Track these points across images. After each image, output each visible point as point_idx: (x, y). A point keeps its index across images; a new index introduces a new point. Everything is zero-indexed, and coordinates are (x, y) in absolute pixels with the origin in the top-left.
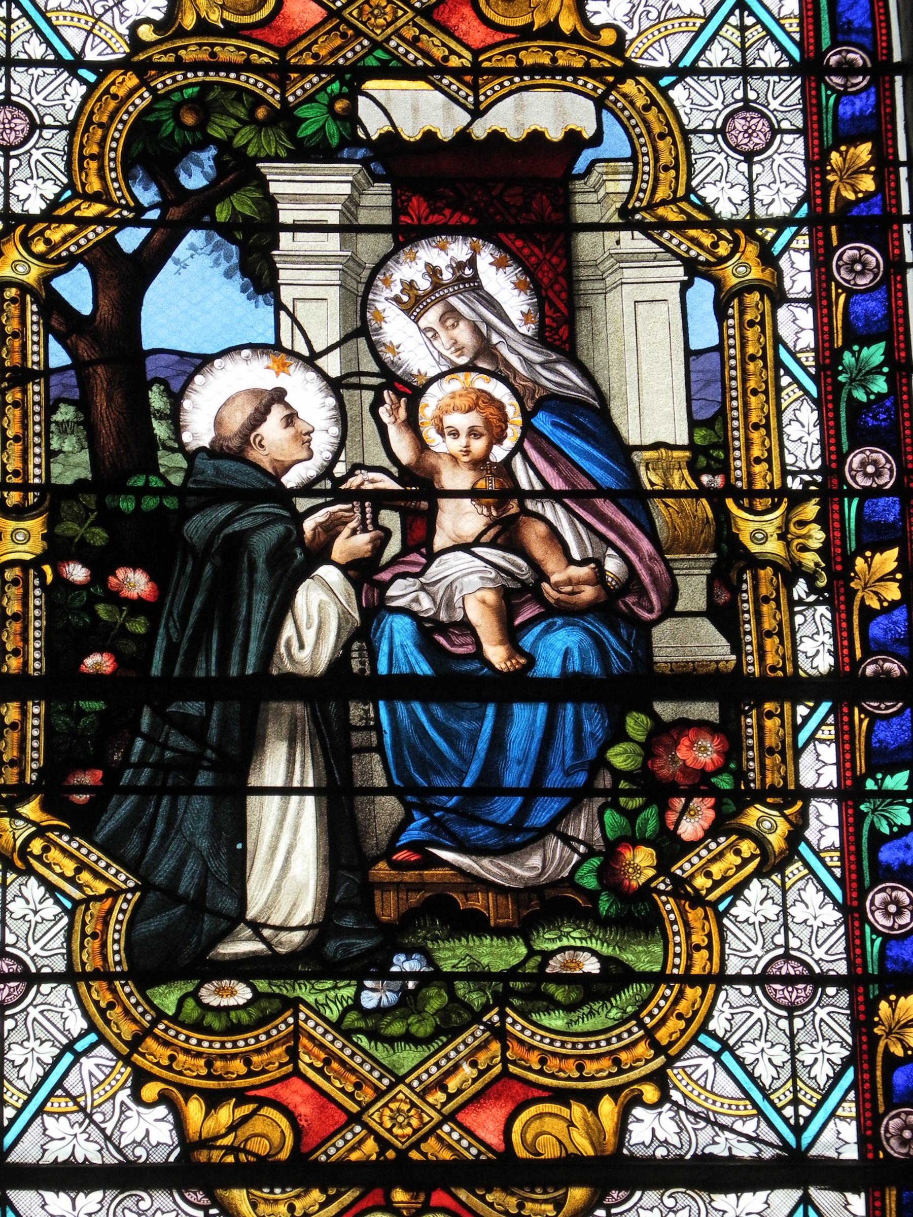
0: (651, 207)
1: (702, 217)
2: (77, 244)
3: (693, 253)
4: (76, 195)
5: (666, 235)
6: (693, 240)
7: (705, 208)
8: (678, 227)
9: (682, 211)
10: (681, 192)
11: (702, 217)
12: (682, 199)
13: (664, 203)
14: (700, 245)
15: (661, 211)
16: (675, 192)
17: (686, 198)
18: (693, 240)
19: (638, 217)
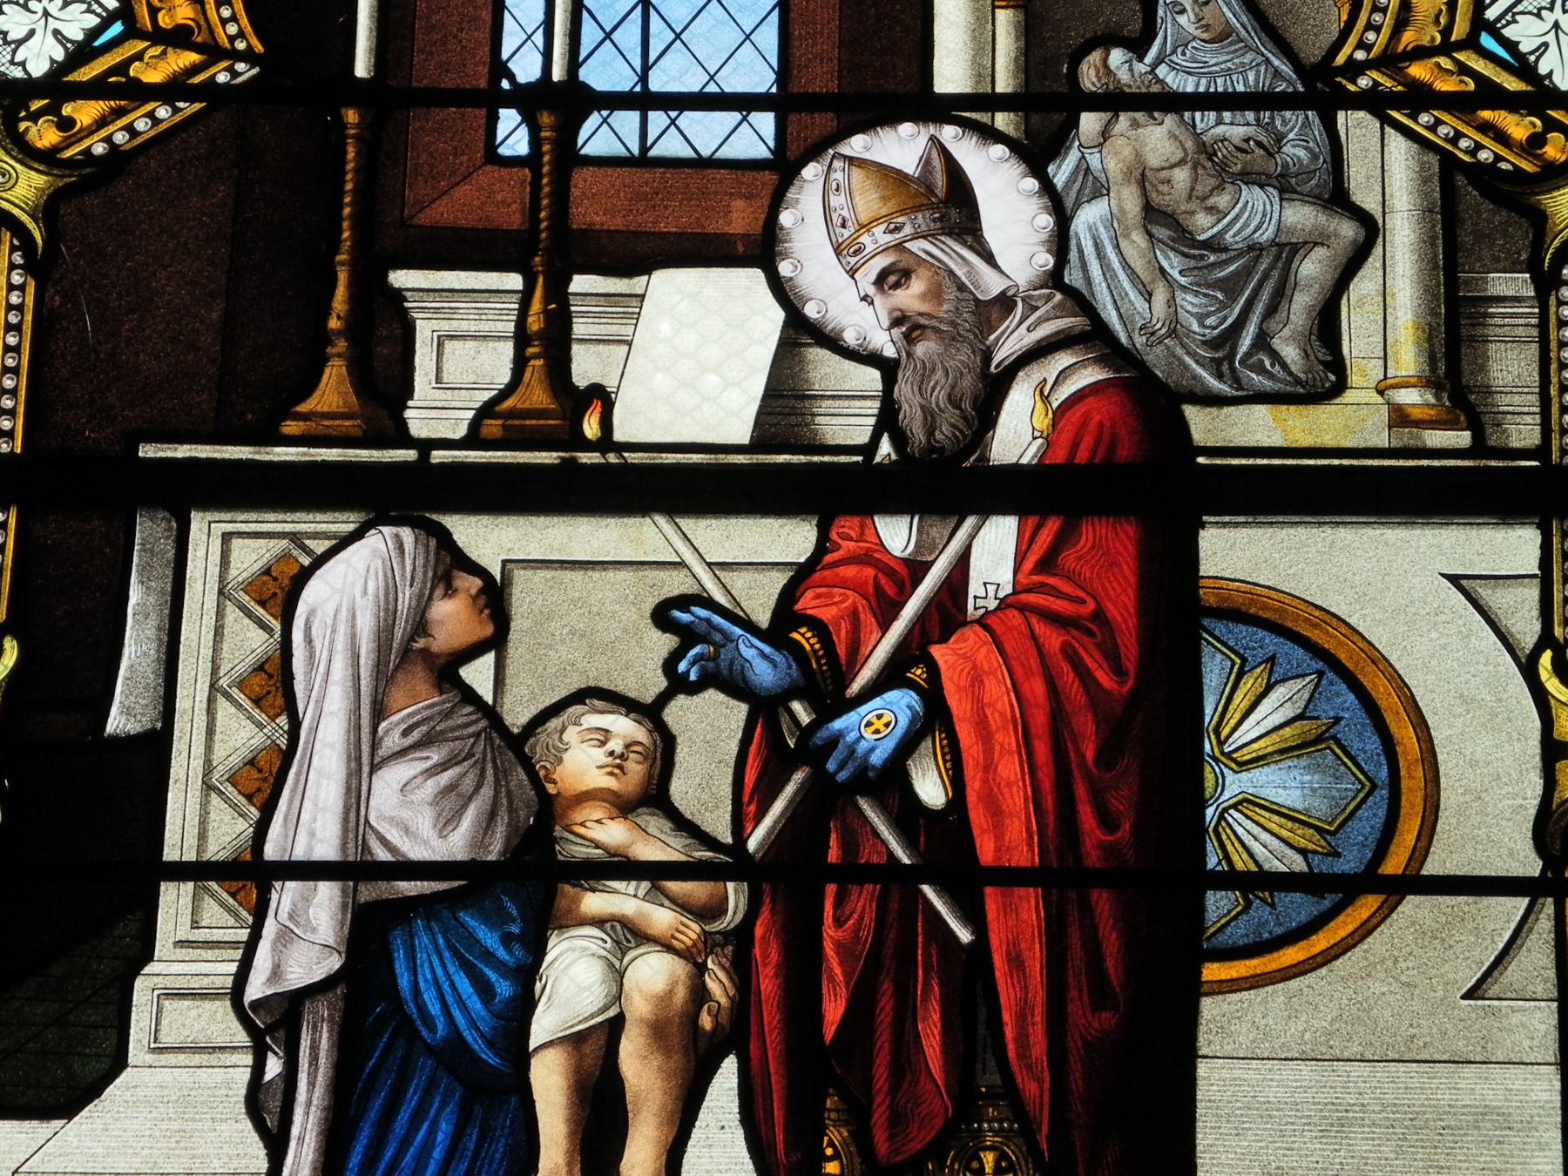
0: (1391, 60)
1: (1512, 84)
2: (129, 129)
3: (1483, 156)
4: (132, 32)
5: (1425, 118)
6: (1486, 128)
7: (1523, 66)
8: (1458, 104)
9: (1464, 70)
10: (1460, 30)
11: (1512, 84)
12: (1461, 45)
13: (1421, 53)
14: (1502, 137)
15: (1418, 71)
16: (1446, 32)
17: (1471, 43)
18: (1486, 128)
19: (1364, 82)
